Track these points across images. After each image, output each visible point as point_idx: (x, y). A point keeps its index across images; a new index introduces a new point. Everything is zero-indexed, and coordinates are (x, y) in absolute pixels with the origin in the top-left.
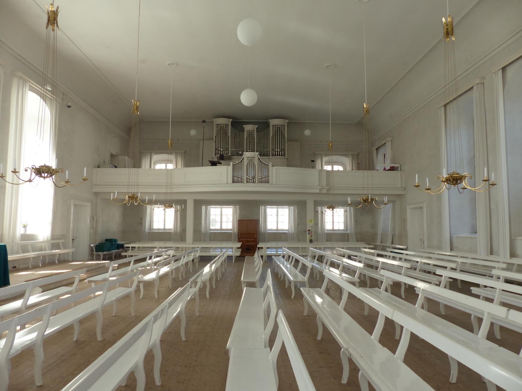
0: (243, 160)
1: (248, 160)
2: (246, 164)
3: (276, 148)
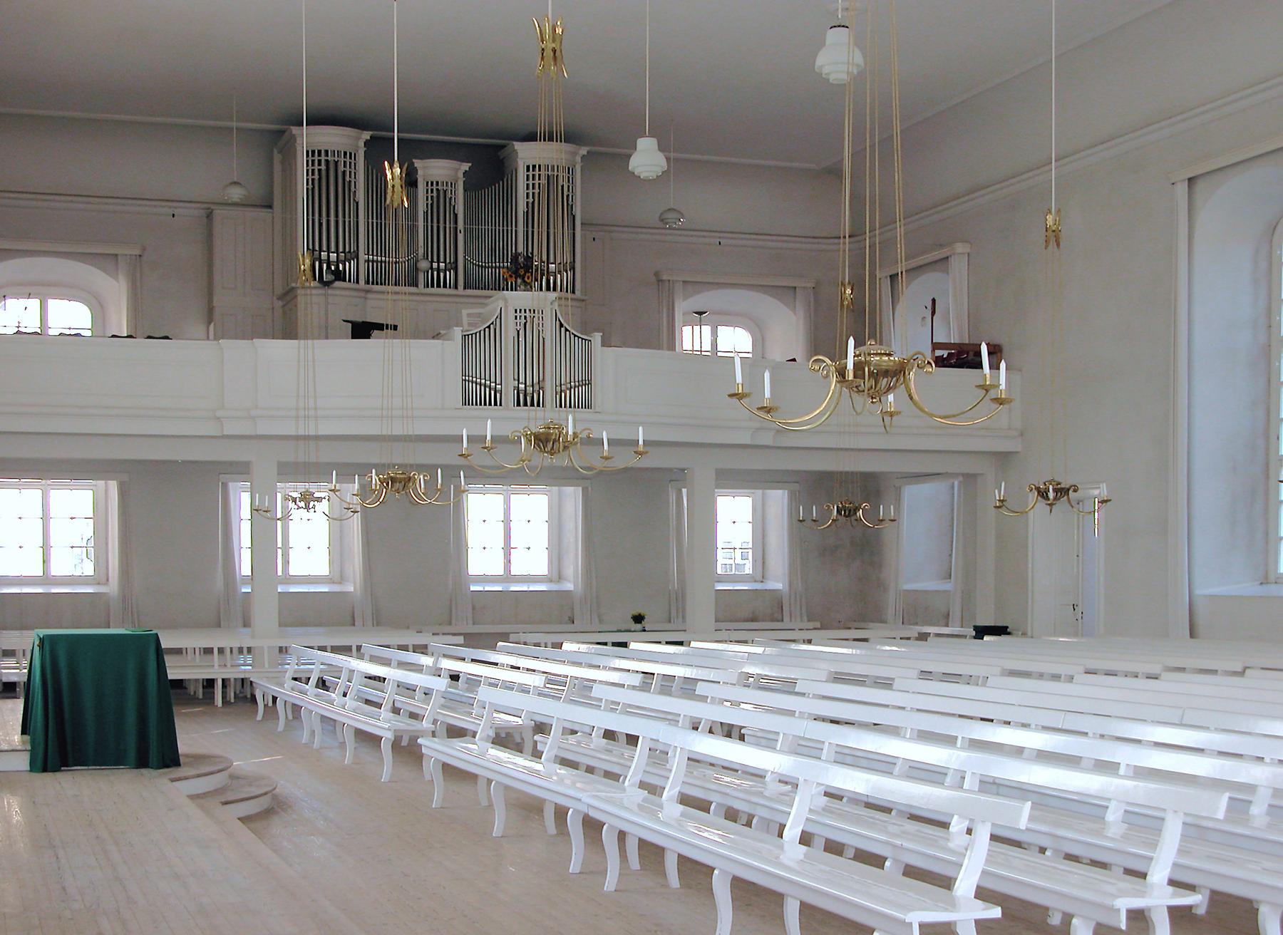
2: (513, 333)
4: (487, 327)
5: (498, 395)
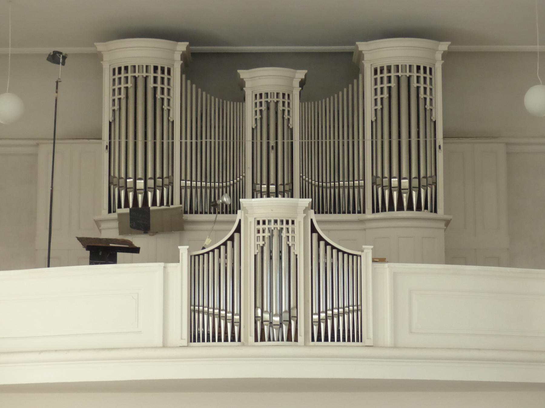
0: (236, 235)
1: (261, 234)
3: (395, 172)
4: (216, 248)
5: (236, 329)
